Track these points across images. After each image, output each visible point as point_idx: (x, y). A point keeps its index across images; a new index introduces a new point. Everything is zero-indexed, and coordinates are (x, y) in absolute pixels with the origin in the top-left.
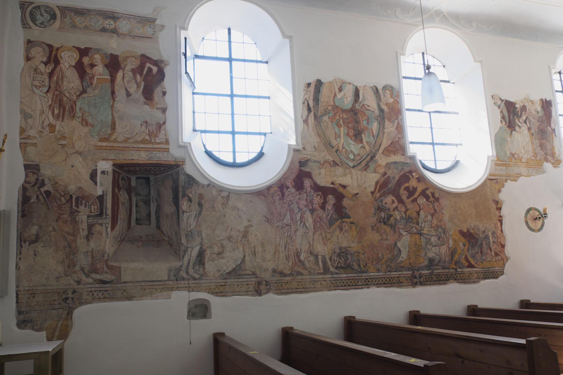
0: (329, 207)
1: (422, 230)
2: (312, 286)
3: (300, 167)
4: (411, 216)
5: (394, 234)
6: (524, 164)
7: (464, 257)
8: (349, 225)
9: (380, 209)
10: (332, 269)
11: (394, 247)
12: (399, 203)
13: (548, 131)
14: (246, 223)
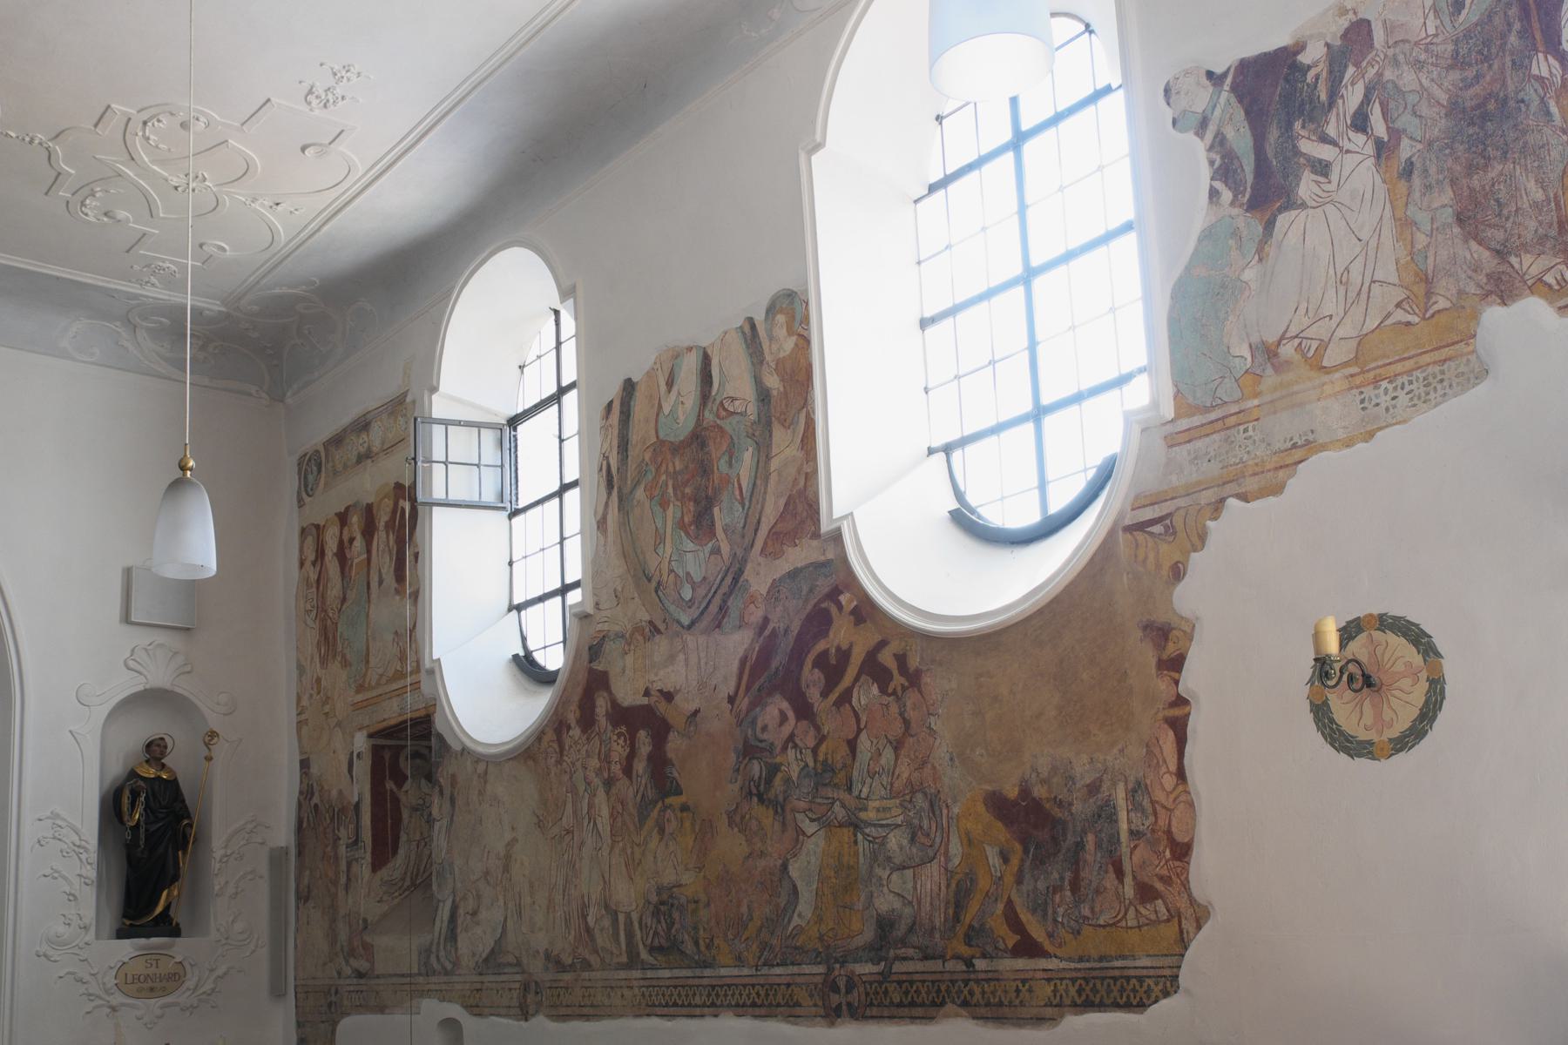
0: (640, 766)
1: (861, 810)
2: (606, 1002)
3: (590, 662)
4: (830, 762)
5: (783, 832)
6: (1337, 375)
7: (1000, 907)
8: (679, 814)
9: (749, 751)
10: (644, 955)
11: (780, 881)
12: (799, 717)
13: (1531, 93)
14: (508, 836)
